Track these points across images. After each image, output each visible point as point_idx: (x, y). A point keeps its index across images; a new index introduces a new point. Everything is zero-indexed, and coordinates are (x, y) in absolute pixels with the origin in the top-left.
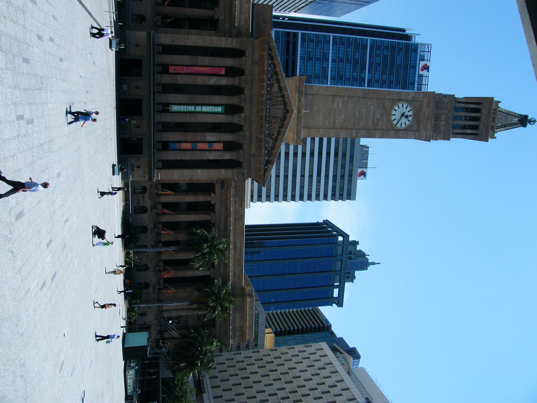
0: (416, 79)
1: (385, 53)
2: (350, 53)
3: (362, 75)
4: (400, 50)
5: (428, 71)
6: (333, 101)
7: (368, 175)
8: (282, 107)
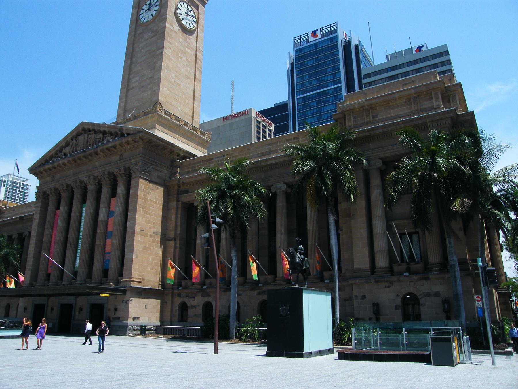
0: (326, 38)
1: (307, 77)
2: (312, 112)
3: (330, 92)
4: (302, 64)
5: (317, 30)
6: (133, 88)
7: (419, 44)
8: (80, 137)
